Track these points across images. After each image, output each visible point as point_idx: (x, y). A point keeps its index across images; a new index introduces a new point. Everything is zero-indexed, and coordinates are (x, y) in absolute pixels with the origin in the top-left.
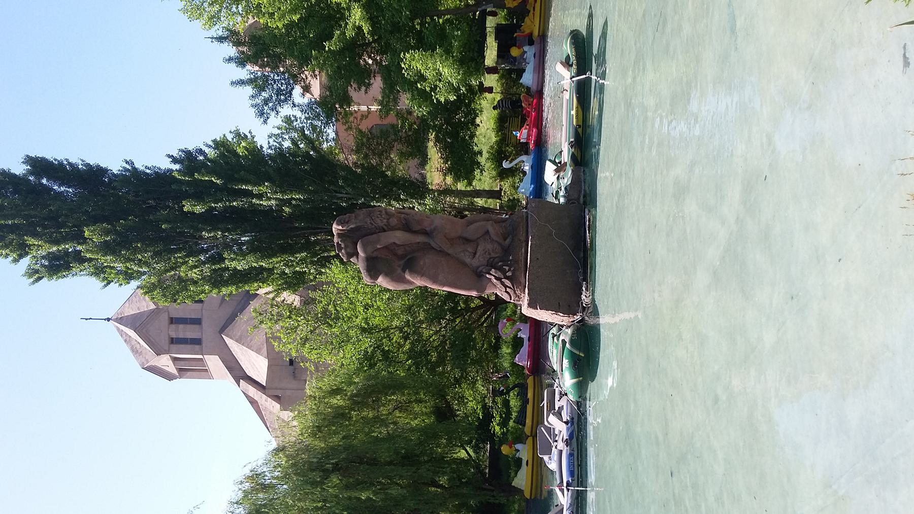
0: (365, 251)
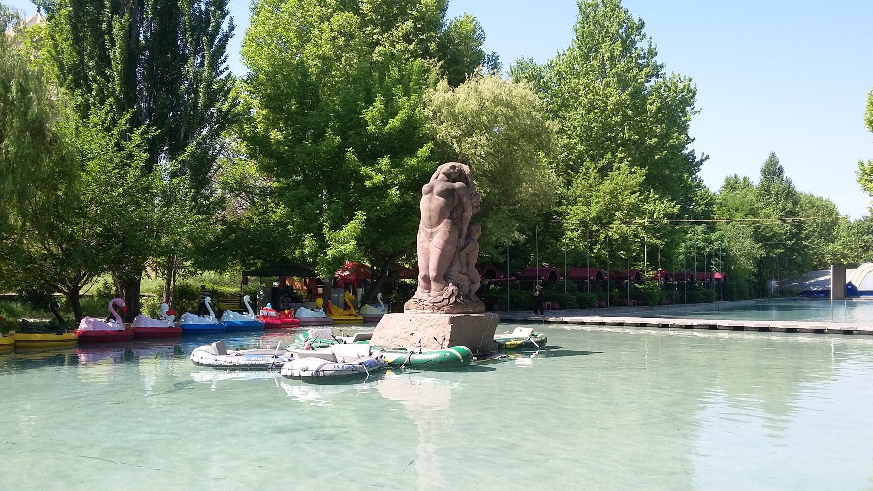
0: (460, 188)
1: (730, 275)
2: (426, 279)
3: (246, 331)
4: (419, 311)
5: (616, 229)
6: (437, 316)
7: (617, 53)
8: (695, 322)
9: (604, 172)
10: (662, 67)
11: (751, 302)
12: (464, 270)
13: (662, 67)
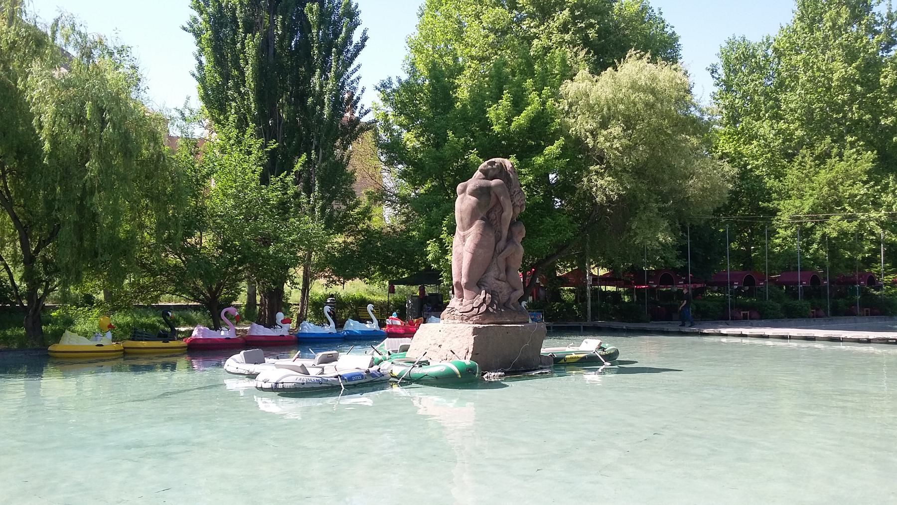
0: (497, 186)
3: (364, 340)
4: (450, 321)
5: (834, 225)
7: (841, 21)
8: (872, 335)
9: (822, 159)
12: (503, 275)
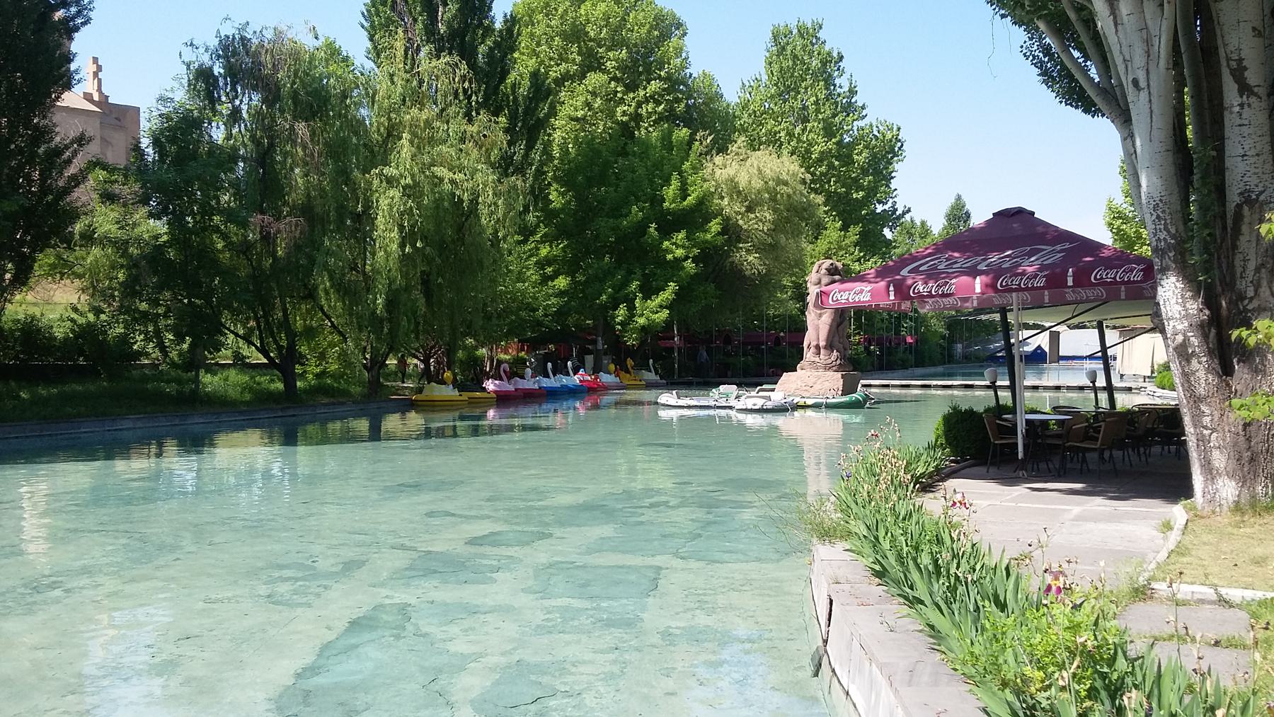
1: (921, 340)
2: (817, 347)
6: (831, 373)
10: (863, 108)
11: (940, 369)
13: (863, 108)
